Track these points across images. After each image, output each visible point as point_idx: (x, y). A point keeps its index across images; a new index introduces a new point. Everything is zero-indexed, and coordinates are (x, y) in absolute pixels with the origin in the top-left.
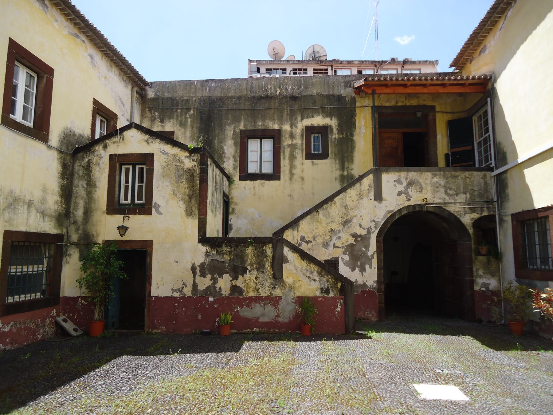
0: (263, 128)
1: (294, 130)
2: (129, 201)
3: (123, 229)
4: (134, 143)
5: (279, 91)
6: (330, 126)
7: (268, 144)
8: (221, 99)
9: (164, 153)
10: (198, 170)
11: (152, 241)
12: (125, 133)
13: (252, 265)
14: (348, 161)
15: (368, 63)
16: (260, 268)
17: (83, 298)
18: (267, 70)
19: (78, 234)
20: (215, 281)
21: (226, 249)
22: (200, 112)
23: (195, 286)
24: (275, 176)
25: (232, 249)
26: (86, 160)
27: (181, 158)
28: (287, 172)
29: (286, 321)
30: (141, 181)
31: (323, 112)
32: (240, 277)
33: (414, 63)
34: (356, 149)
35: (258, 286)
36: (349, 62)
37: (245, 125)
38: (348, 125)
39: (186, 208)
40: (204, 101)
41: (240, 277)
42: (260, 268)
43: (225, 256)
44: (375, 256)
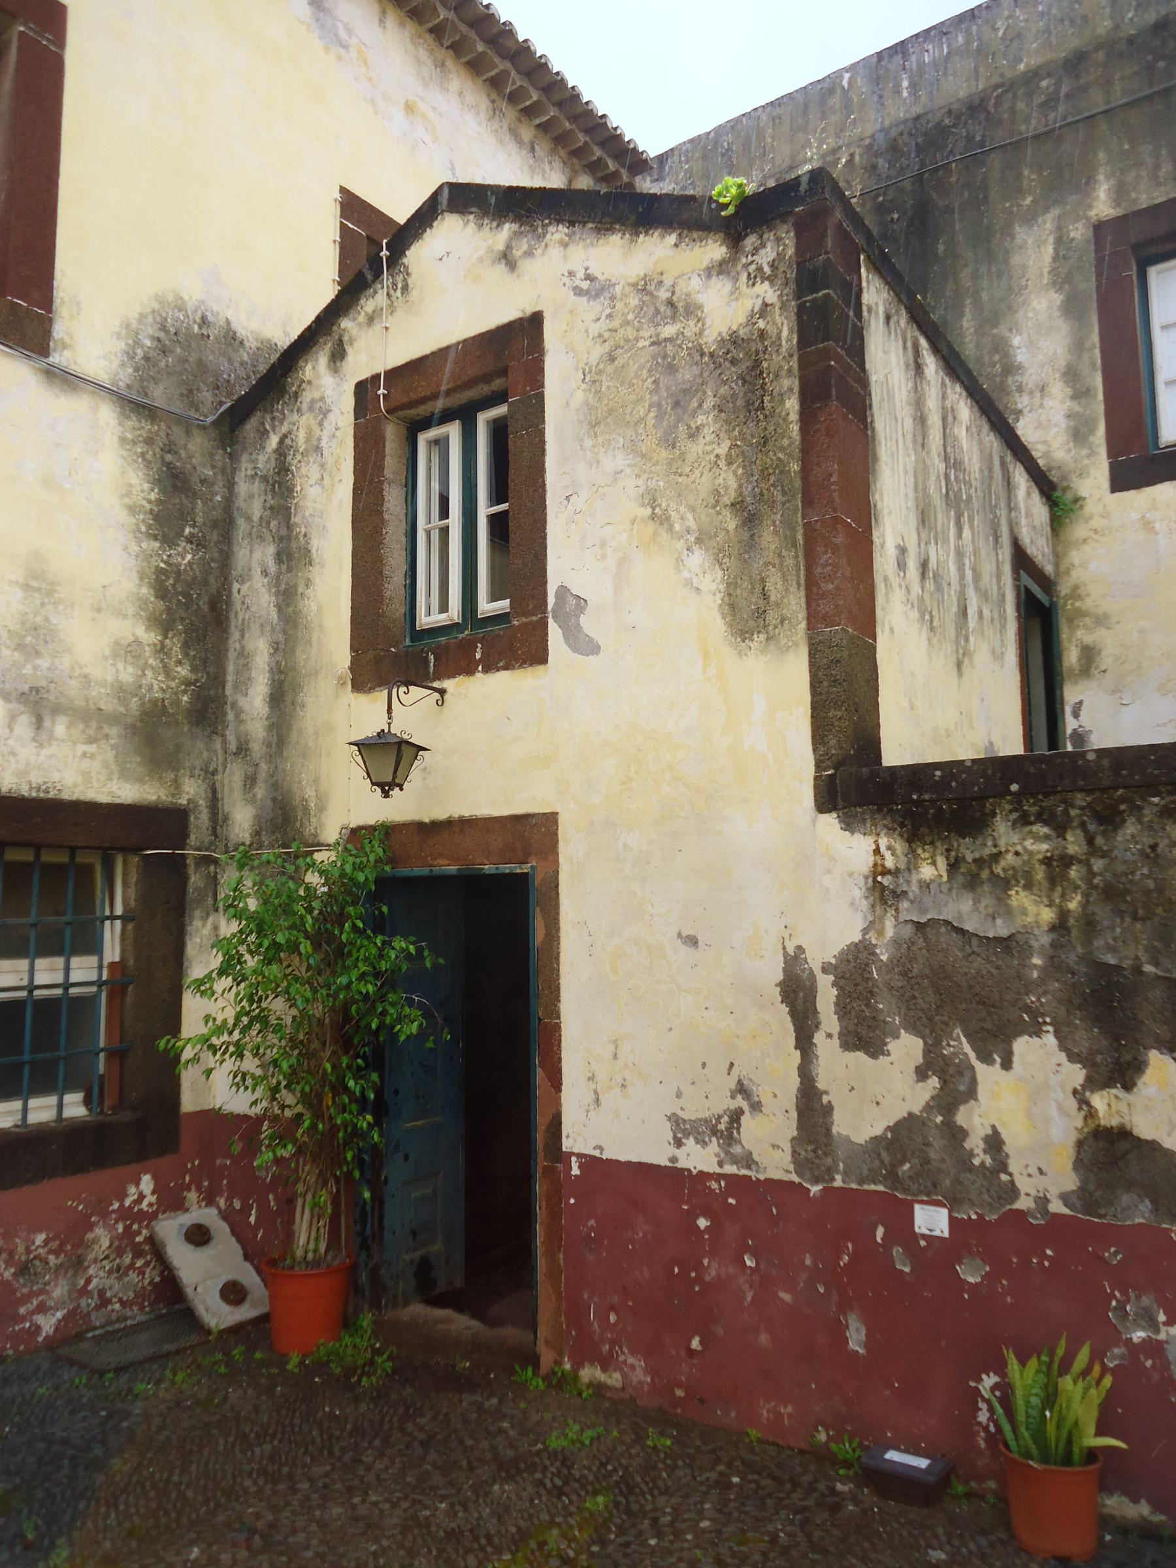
2: (455, 611)
8: (976, 108)
9: (593, 288)
10: (784, 328)
11: (551, 819)
19: (252, 801)
20: (955, 1089)
21: (1017, 842)
23: (812, 1108)
25: (1074, 844)
26: (273, 441)
27: (682, 287)
37: (1120, 192)
39: (731, 586)
43: (1019, 898)
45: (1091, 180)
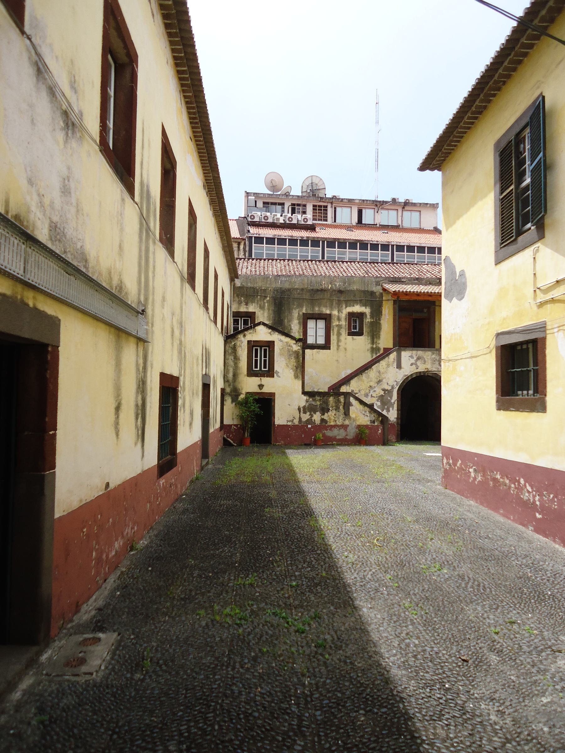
0: (319, 312)
1: (340, 315)
2: (258, 369)
3: (261, 386)
4: (262, 334)
5: (330, 286)
6: (365, 313)
7: (321, 324)
8: (289, 290)
9: (281, 341)
10: (301, 352)
13: (332, 407)
14: (376, 338)
15: (368, 202)
16: (337, 409)
17: (235, 425)
18: (264, 203)
20: (312, 416)
21: (318, 398)
22: (274, 299)
23: (300, 419)
24: (326, 346)
26: (233, 343)
29: (352, 438)
30: (265, 356)
32: (326, 414)
33: (414, 204)
34: (382, 330)
35: (336, 419)
36: (350, 201)
37: (306, 310)
38: (377, 313)
40: (277, 291)
41: (326, 414)
42: (337, 409)
44: (396, 402)
45: (303, 307)
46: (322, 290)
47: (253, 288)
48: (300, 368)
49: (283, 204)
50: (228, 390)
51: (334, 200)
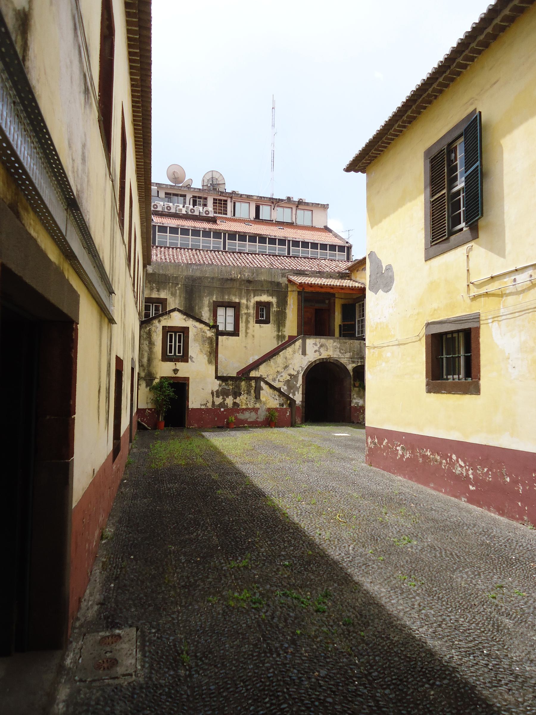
0: (228, 300)
1: (249, 303)
2: (173, 354)
3: (176, 371)
4: (177, 320)
5: (239, 276)
7: (231, 312)
8: (200, 278)
9: (195, 327)
12: (171, 314)
13: (244, 391)
14: (282, 326)
15: (266, 199)
16: (249, 393)
17: (149, 409)
18: (166, 194)
21: (230, 382)
22: (186, 286)
23: (213, 402)
24: (235, 333)
26: (148, 329)
28: (244, 331)
29: (262, 420)
30: (180, 342)
31: (268, 293)
33: (307, 204)
35: (248, 403)
36: (249, 197)
37: (216, 298)
38: (283, 303)
40: (188, 278)
42: (249, 393)
44: (301, 387)
46: (231, 279)
47: (165, 275)
48: (214, 354)
49: (184, 196)
50: (143, 374)
51: (233, 195)
